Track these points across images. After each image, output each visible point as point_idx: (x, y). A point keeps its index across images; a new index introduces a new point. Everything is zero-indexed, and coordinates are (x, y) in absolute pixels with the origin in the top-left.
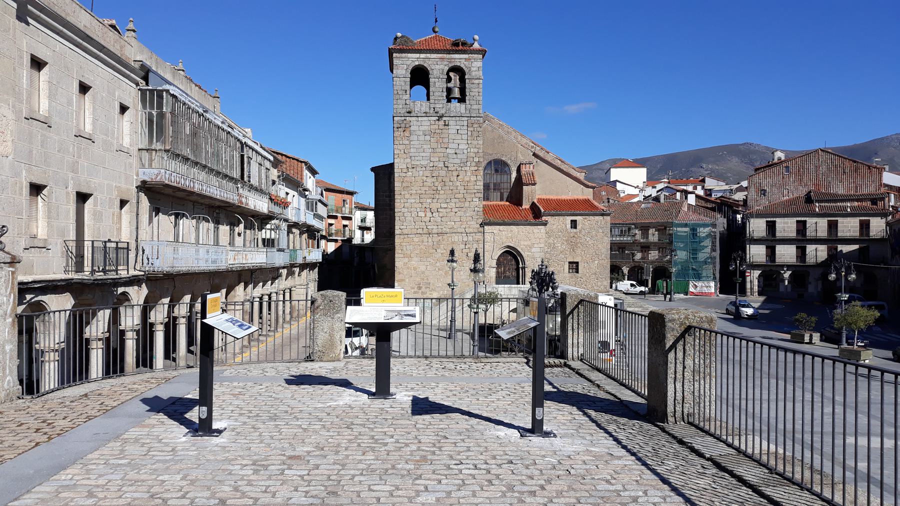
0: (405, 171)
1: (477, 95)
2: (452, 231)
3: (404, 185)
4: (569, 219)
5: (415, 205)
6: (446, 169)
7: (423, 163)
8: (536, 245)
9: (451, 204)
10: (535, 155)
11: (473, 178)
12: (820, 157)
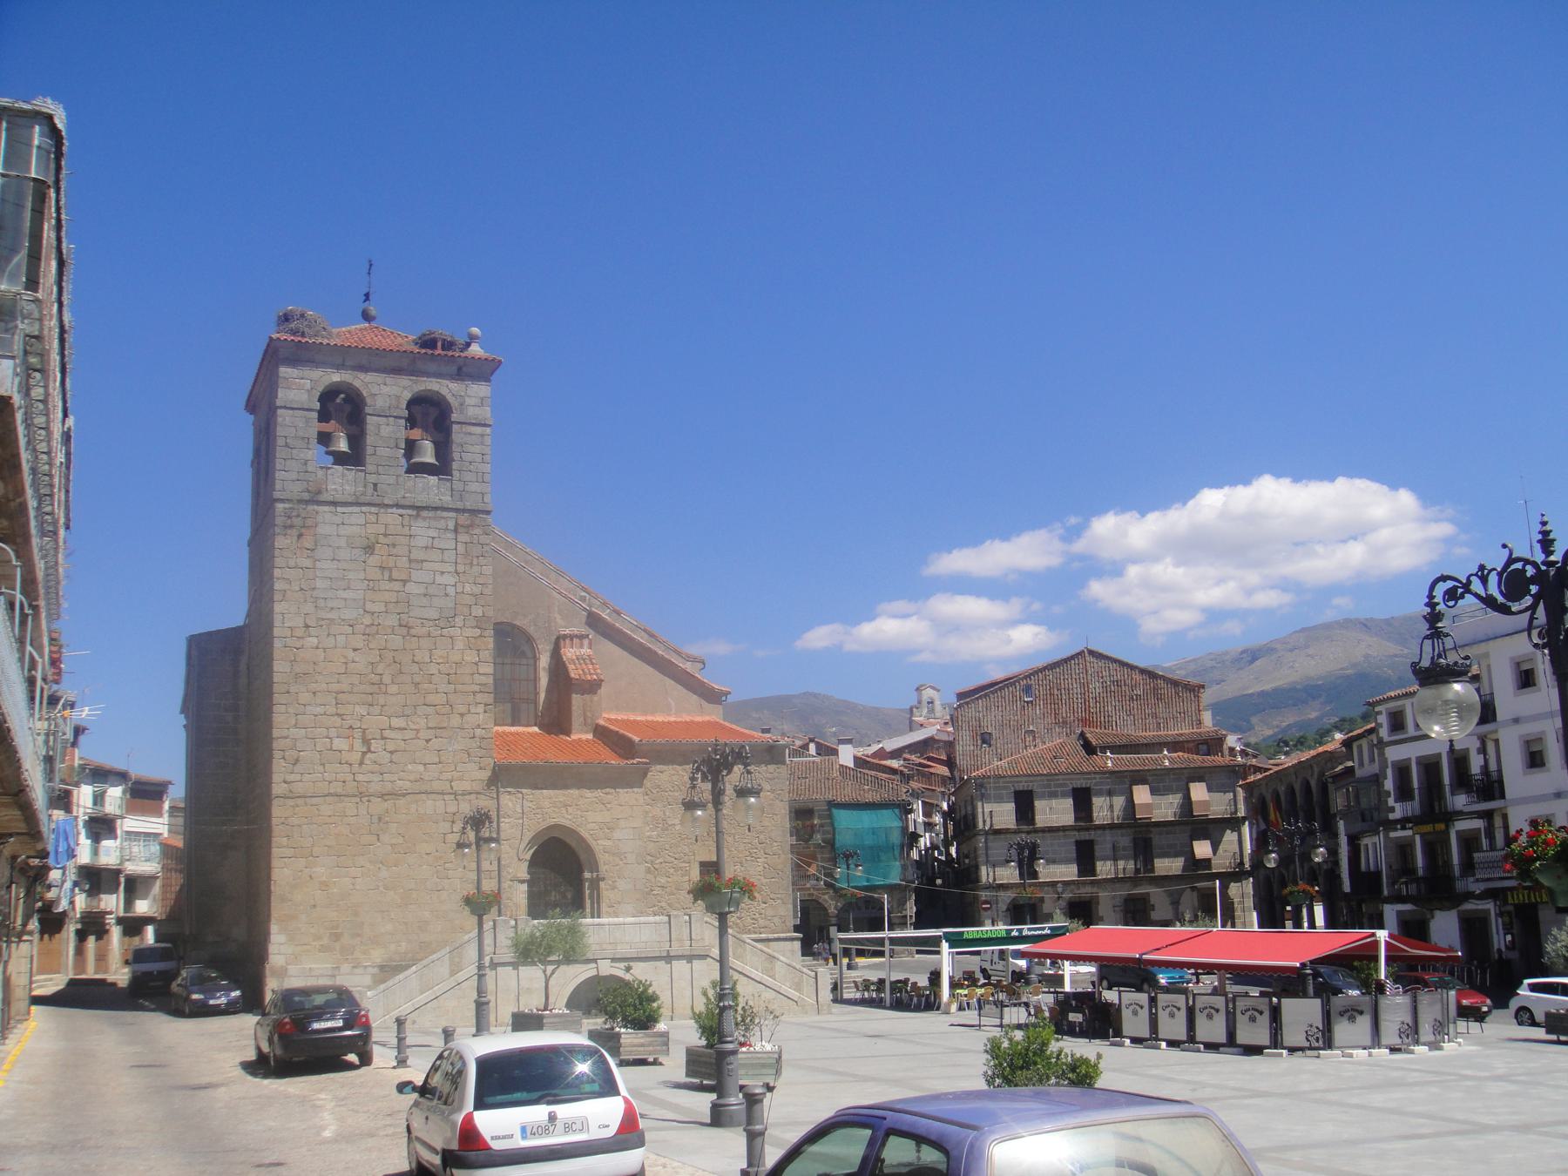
0: (299, 633)
1: (478, 458)
6: (404, 631)
7: (349, 614)
8: (622, 823)
11: (471, 657)
12: (1088, 664)
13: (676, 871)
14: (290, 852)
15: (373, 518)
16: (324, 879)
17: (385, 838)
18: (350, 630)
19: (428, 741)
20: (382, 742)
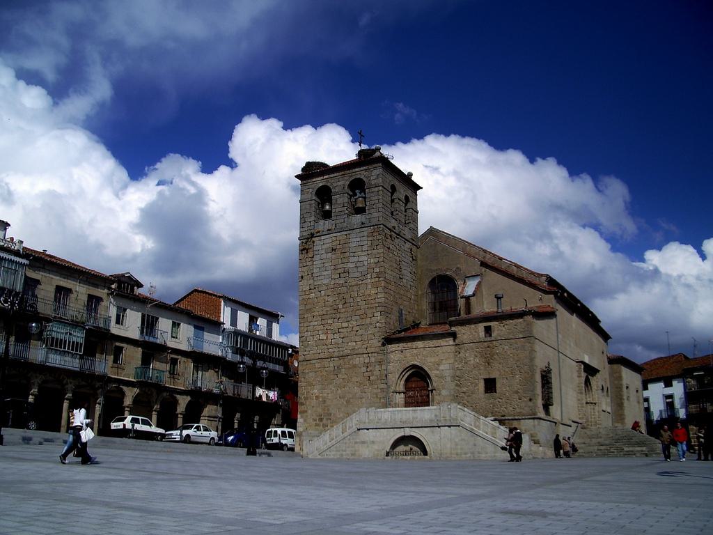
2: (352, 352)
3: (307, 307)
5: (318, 328)
7: (325, 282)
8: (444, 362)
9: (351, 322)
10: (483, 264)
13: (472, 384)
14: (304, 384)
17: (340, 376)
20: (338, 334)
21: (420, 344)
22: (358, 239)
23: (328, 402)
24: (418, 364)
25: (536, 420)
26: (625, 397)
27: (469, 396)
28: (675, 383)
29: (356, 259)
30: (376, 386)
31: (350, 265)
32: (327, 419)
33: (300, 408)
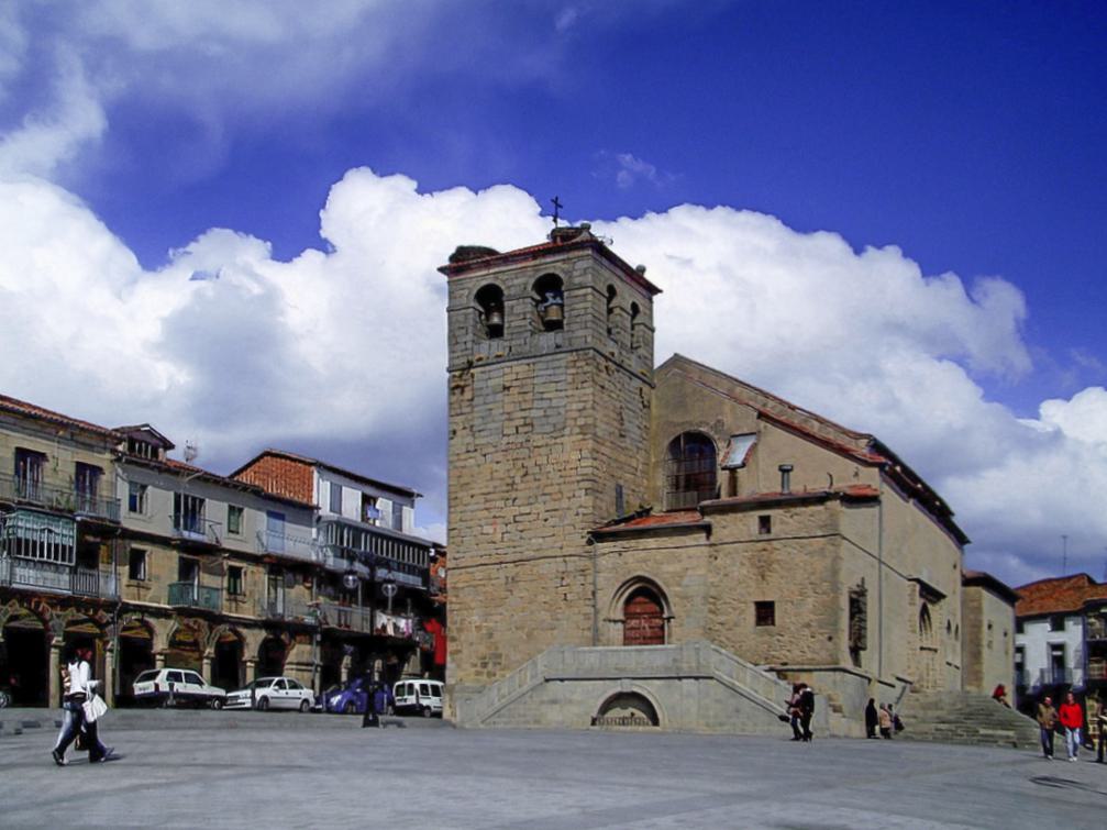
2: (538, 555)
3: (462, 481)
4: (755, 515)
8: (690, 572)
11: (575, 456)
13: (735, 609)
14: (457, 607)
15: (507, 370)
16: (478, 624)
18: (493, 450)
19: (546, 520)
21: (651, 542)
22: (549, 372)
23: (497, 636)
24: (647, 575)
25: (837, 673)
26: (985, 643)
27: (730, 629)
28: (1069, 624)
29: (545, 404)
30: (576, 610)
31: (534, 413)
32: (495, 664)
33: (451, 646)
